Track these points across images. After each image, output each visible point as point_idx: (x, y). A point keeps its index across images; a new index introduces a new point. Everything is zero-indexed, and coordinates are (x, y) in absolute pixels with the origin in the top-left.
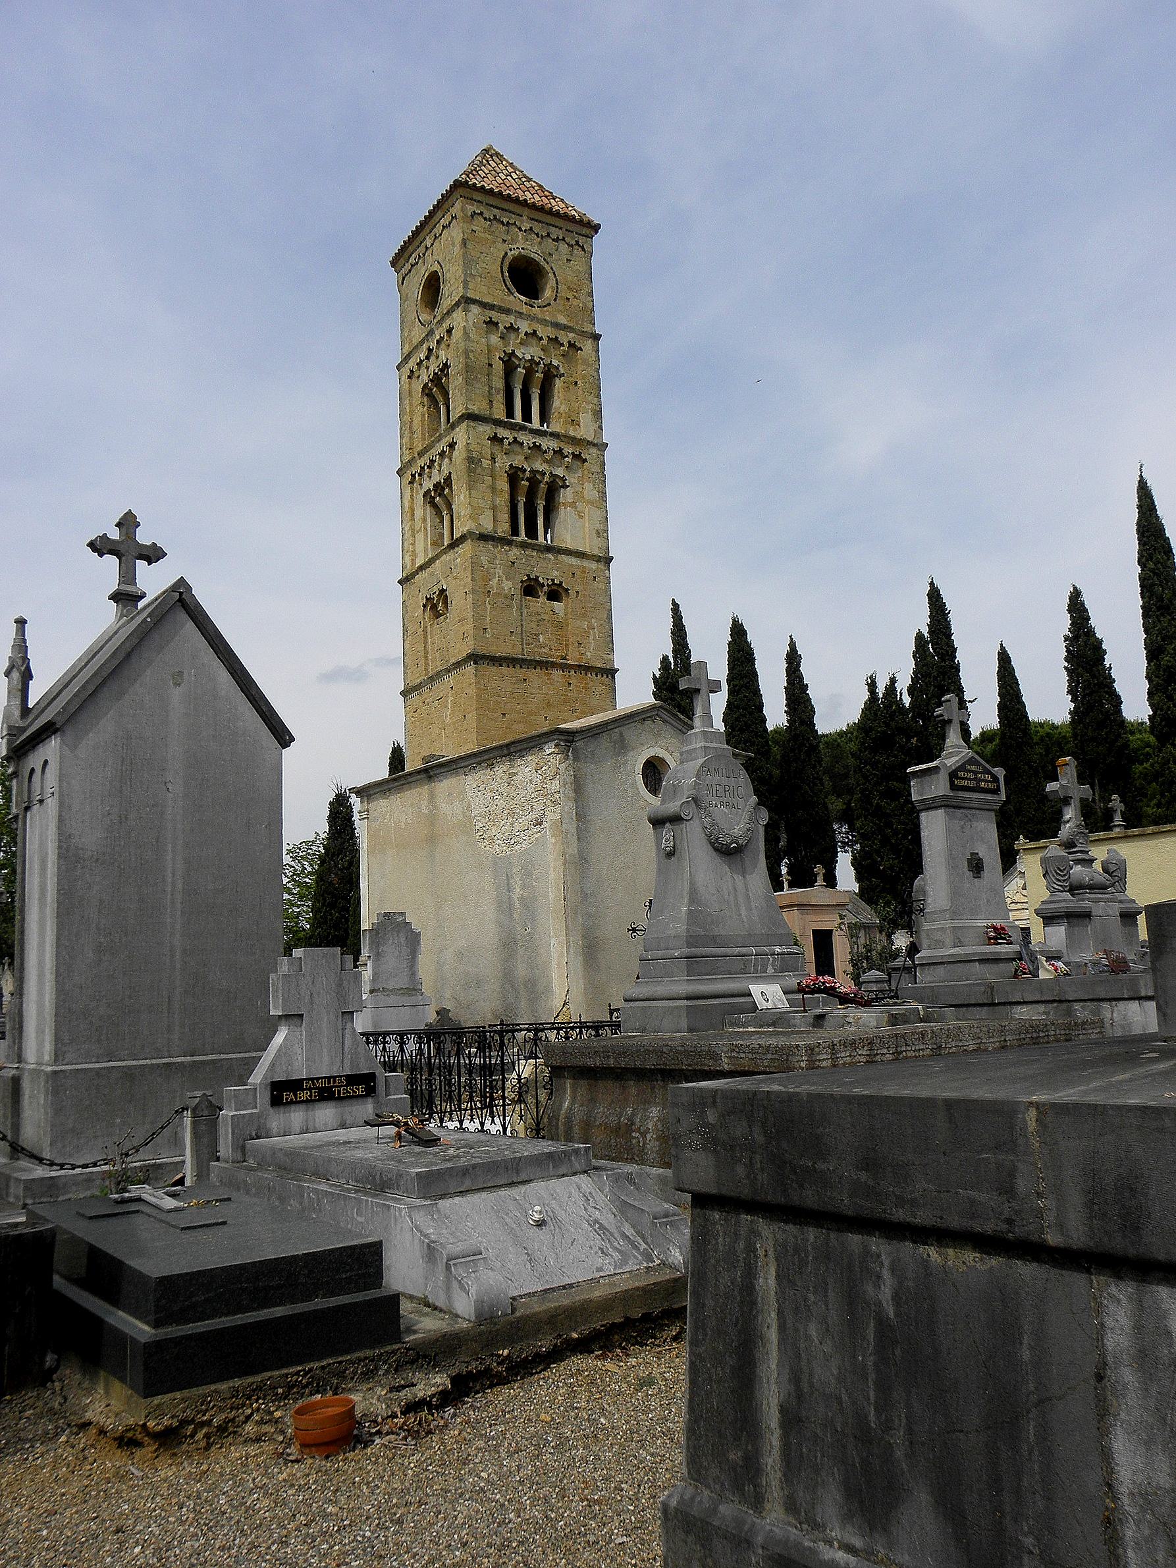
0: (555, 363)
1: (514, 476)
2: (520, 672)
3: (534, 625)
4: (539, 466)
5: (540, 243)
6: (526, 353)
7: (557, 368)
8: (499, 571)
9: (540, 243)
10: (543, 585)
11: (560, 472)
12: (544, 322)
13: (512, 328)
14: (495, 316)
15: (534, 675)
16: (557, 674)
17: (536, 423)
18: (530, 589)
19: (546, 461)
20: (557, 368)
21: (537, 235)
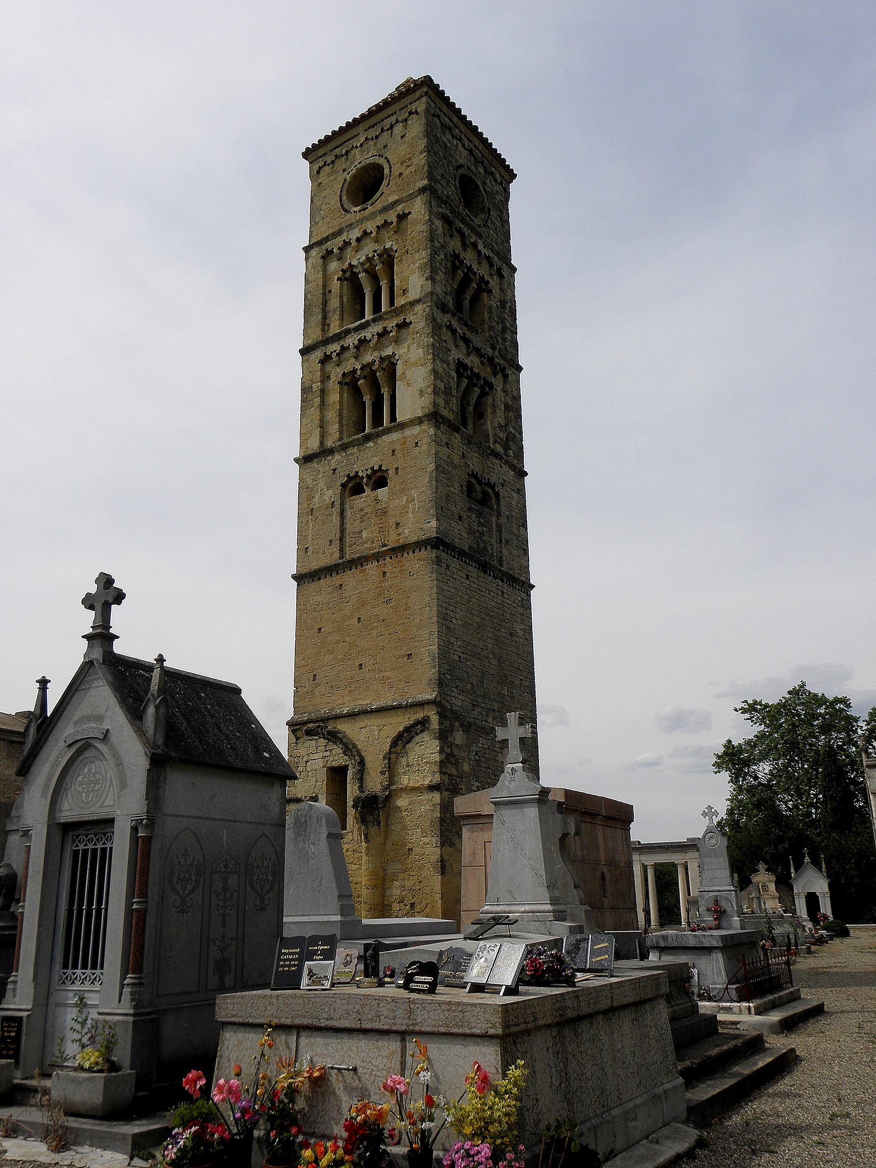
0: (388, 246)
1: (350, 382)
2: (336, 579)
3: (357, 523)
4: (368, 358)
5: (375, 144)
6: (356, 259)
7: (391, 249)
8: (322, 485)
9: (375, 144)
10: (363, 477)
11: (388, 352)
12: (373, 216)
13: (347, 244)
14: (329, 245)
15: (350, 578)
16: (372, 568)
17: (368, 316)
18: (354, 486)
19: (375, 349)
20: (391, 249)
21: (372, 139)
